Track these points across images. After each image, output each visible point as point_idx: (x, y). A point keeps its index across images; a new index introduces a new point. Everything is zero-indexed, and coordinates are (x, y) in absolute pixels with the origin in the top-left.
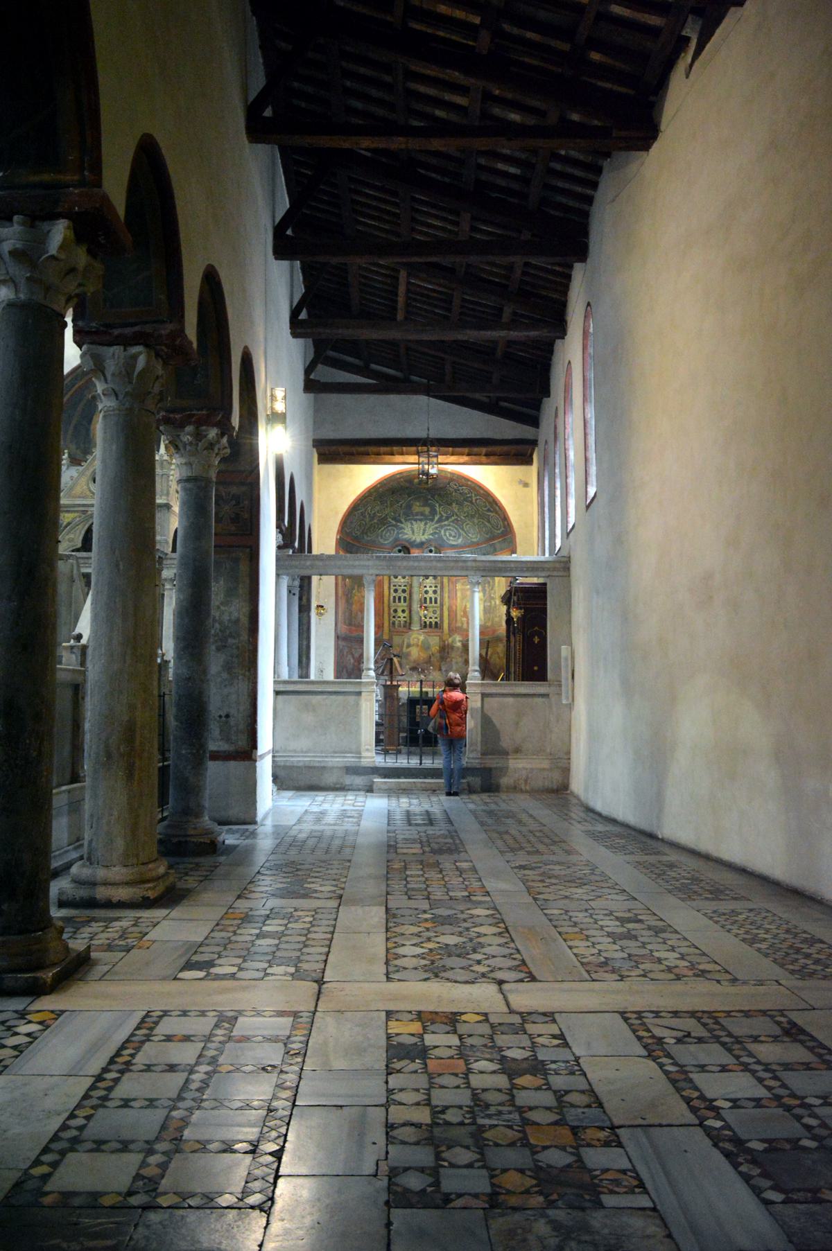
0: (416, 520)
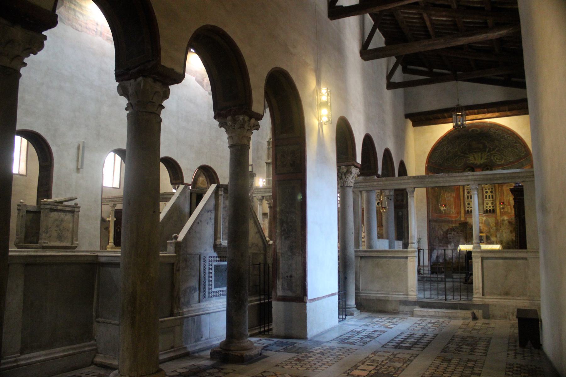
0: (475, 152)
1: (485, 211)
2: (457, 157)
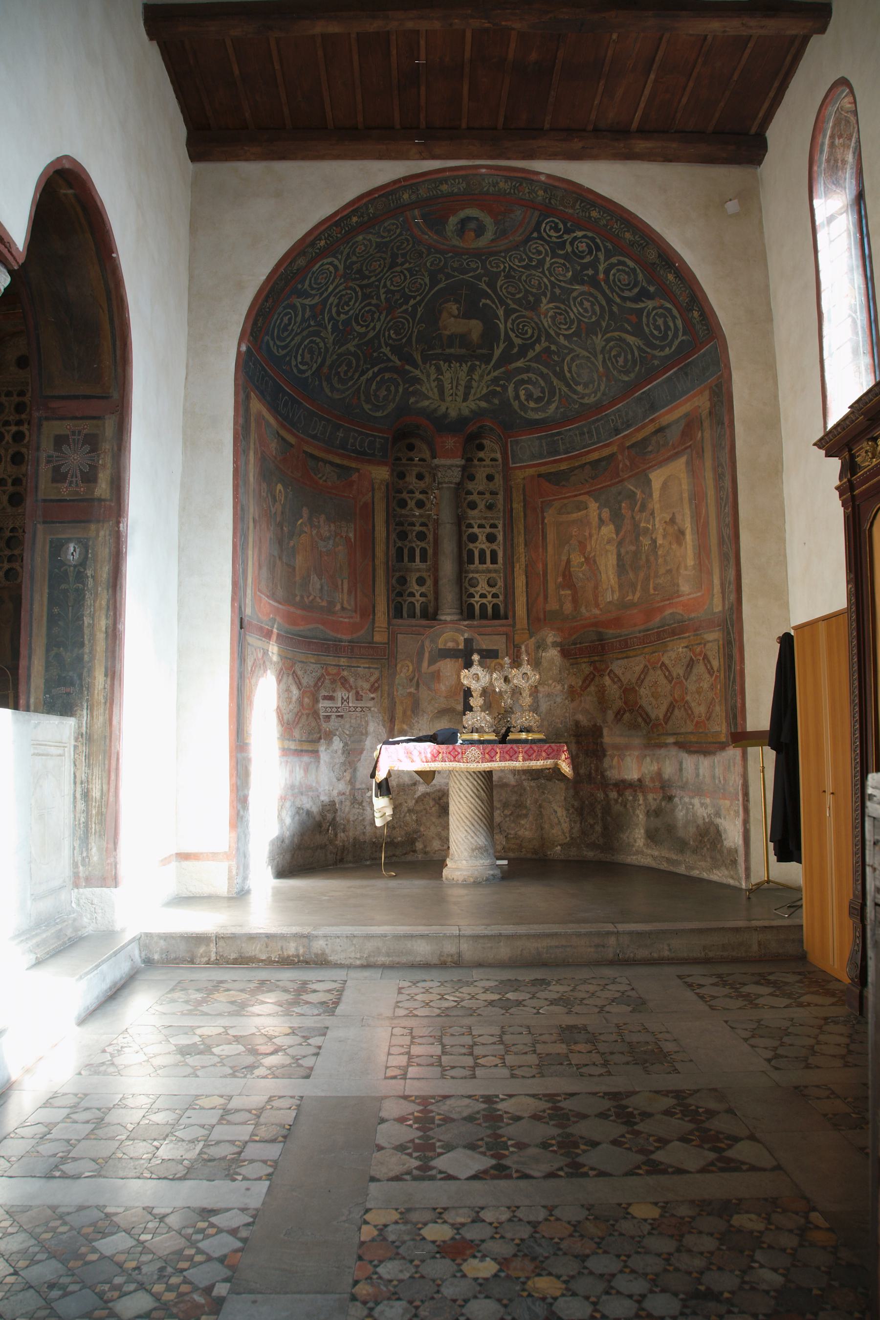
0: (448, 359)
1: (465, 613)
2: (376, 369)
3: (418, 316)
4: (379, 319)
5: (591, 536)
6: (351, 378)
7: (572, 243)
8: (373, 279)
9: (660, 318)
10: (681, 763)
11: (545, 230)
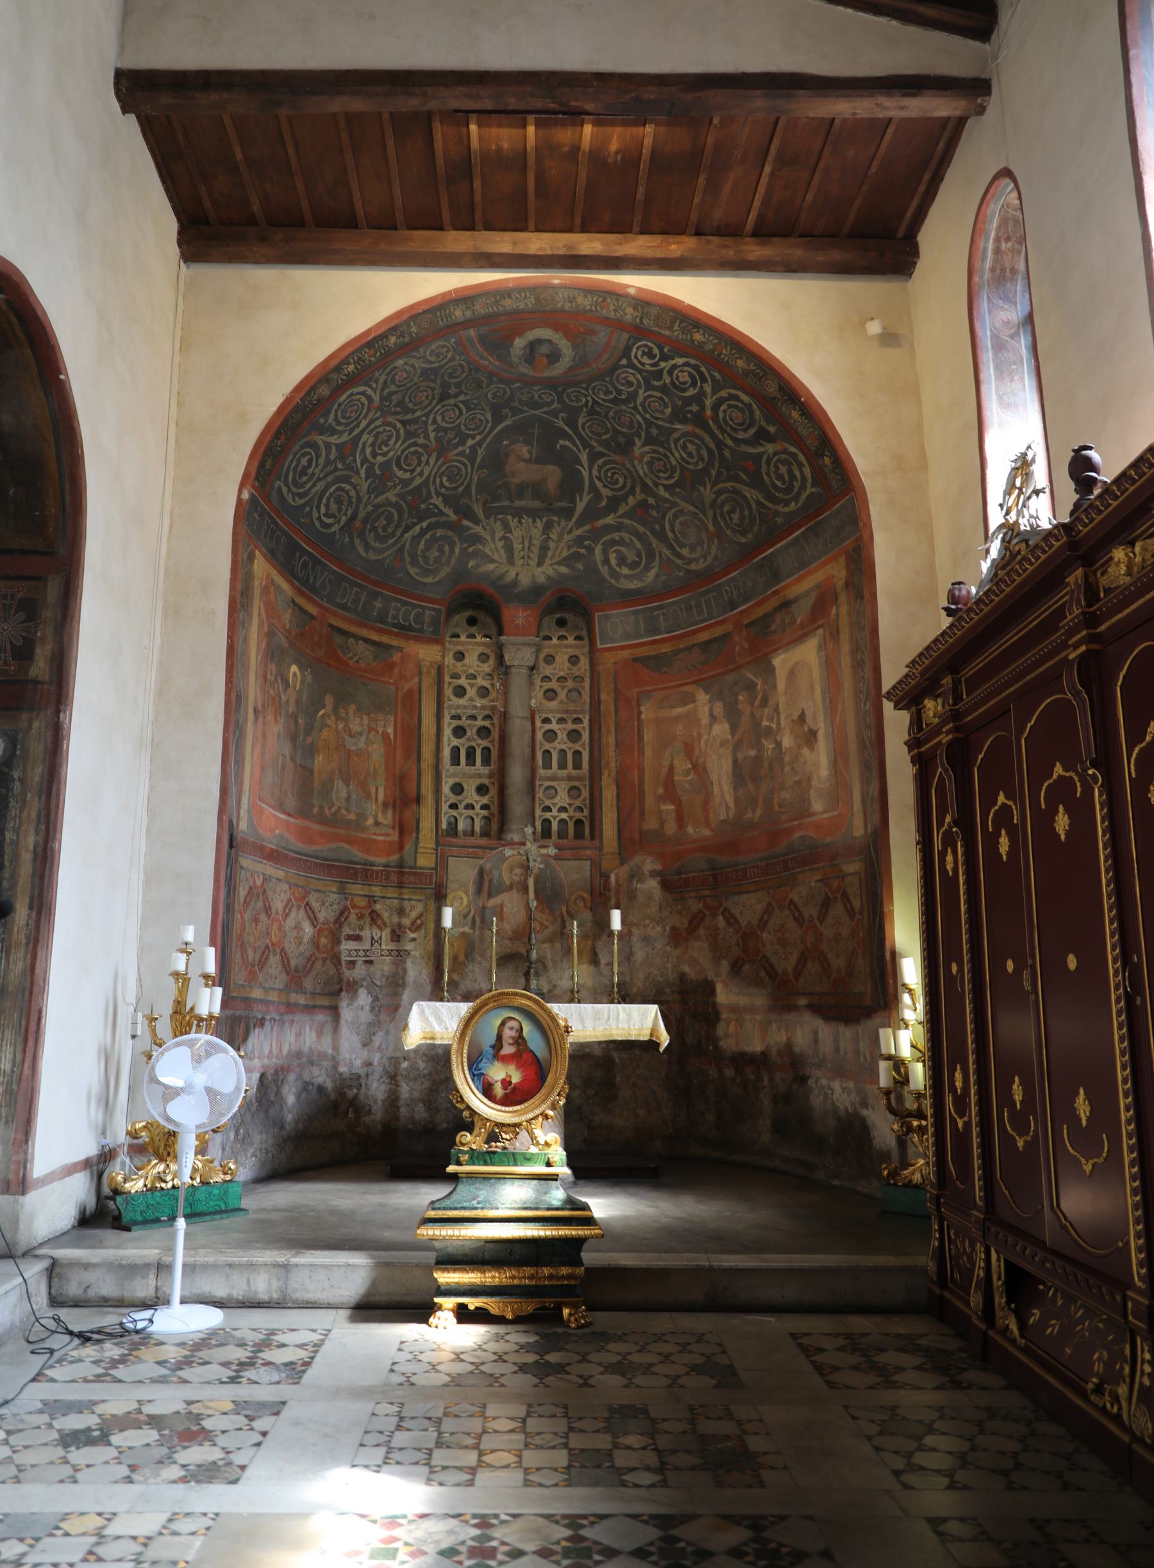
0: (518, 513)
2: (424, 524)
3: (479, 460)
4: (428, 463)
5: (700, 736)
6: (392, 535)
7: (670, 372)
8: (418, 414)
9: (783, 465)
10: (816, 1033)
11: (636, 357)
